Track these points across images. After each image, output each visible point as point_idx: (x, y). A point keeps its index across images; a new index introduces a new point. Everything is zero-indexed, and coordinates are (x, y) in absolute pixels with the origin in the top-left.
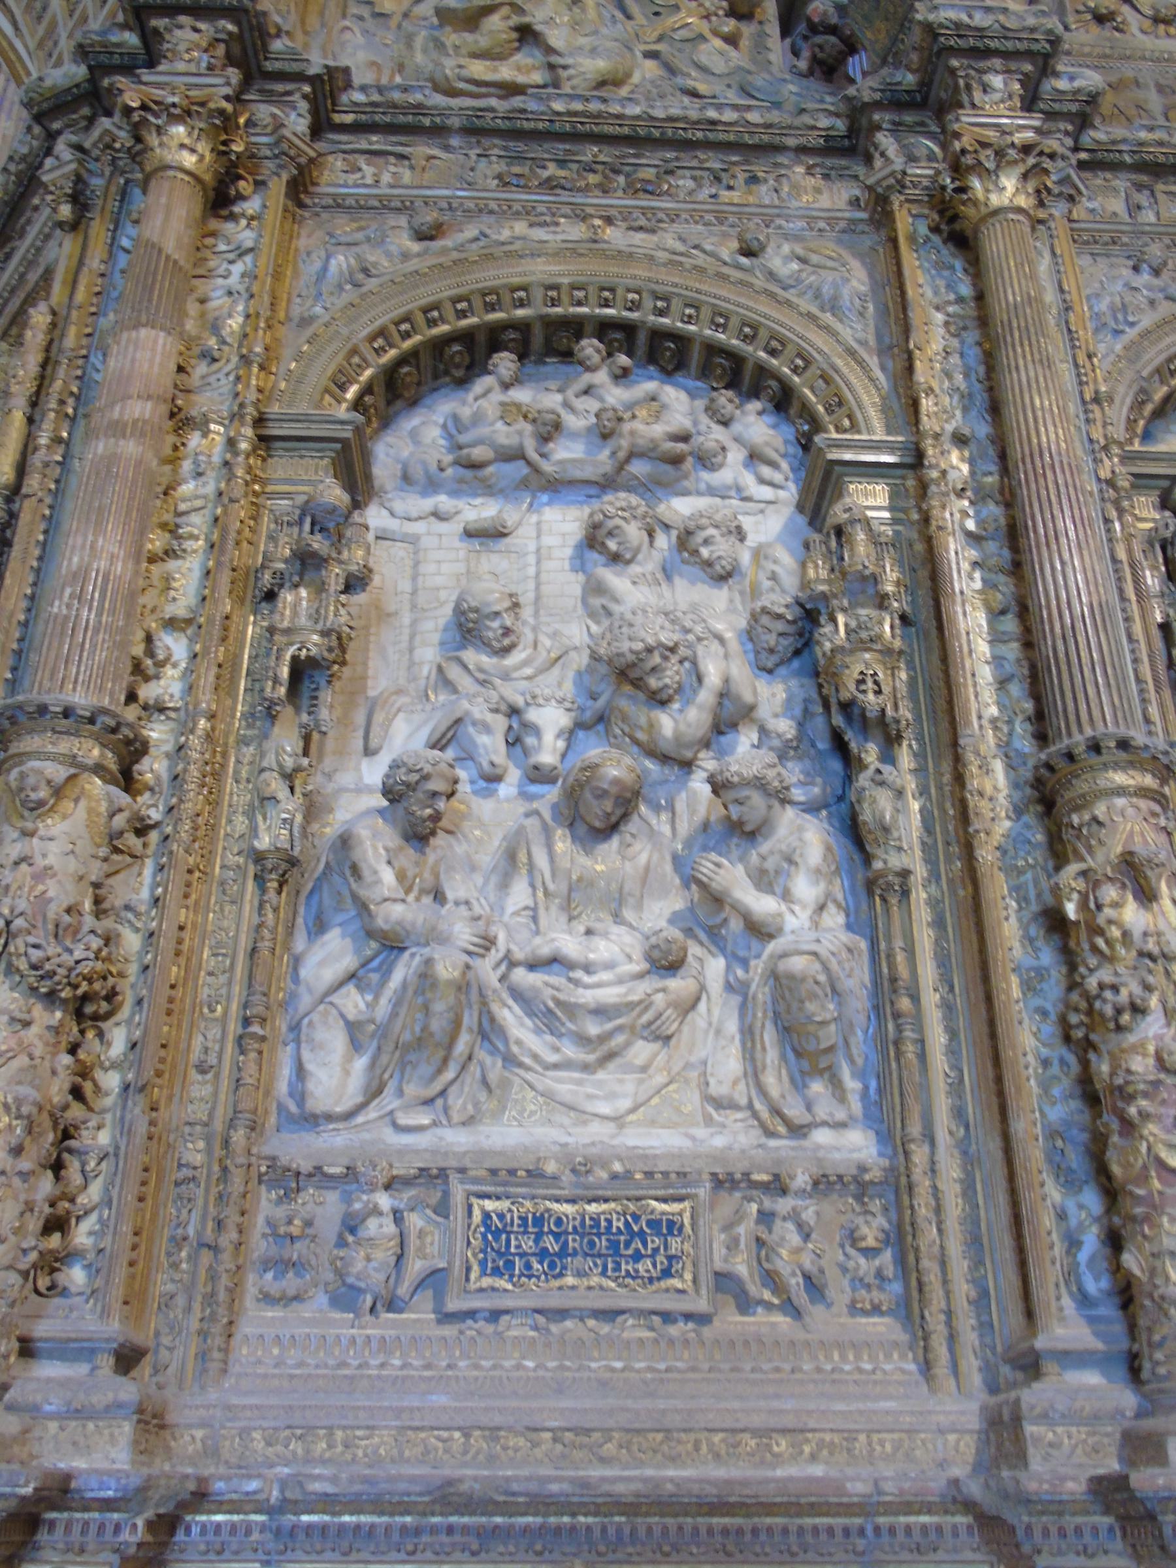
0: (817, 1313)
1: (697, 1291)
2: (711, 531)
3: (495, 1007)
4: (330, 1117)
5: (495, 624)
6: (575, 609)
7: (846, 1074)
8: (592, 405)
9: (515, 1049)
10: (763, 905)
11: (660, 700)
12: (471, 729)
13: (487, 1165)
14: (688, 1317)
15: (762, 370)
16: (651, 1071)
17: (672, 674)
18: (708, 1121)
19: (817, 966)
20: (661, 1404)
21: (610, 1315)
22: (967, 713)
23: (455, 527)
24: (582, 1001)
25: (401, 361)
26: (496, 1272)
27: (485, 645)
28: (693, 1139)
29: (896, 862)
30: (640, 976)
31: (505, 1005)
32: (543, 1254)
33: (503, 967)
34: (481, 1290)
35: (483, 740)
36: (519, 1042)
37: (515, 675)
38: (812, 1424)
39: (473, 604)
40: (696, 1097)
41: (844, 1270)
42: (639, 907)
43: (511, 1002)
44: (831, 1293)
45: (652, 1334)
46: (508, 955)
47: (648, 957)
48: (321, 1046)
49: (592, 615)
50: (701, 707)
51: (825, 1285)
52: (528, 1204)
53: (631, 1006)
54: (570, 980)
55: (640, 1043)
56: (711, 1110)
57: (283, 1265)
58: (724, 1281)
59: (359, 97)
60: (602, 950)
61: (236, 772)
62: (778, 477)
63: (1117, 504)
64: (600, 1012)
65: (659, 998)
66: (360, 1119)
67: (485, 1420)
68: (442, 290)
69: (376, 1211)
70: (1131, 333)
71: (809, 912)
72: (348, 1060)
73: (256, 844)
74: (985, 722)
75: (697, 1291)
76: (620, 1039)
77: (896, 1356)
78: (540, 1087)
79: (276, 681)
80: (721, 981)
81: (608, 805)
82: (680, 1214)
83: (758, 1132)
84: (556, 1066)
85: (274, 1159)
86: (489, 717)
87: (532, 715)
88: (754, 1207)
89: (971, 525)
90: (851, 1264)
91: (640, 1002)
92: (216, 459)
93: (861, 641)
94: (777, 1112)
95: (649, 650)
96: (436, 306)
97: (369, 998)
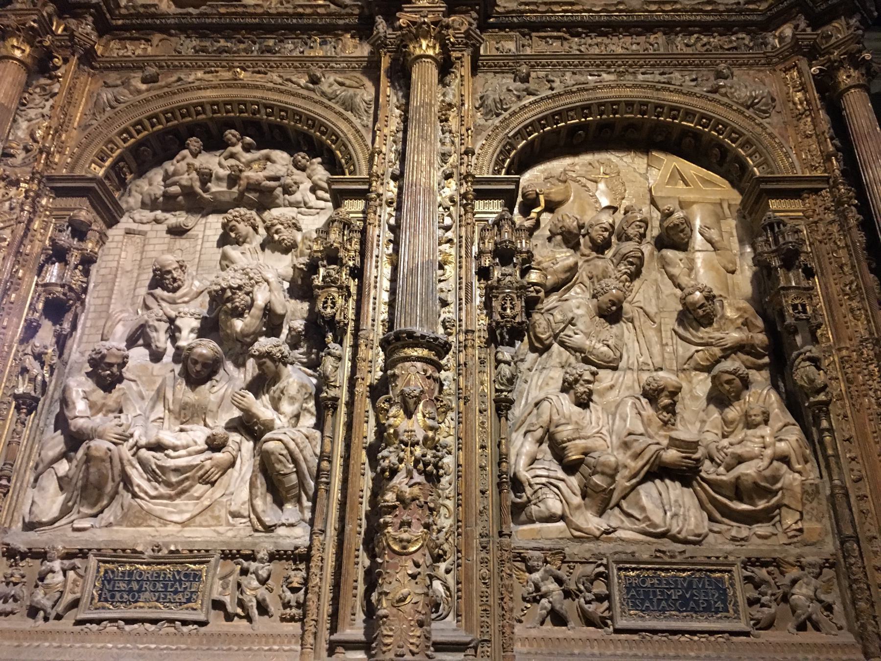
2: (279, 226)
3: (129, 469)
4: (41, 524)
5: (169, 276)
6: (216, 267)
7: (304, 498)
8: (232, 162)
9: (136, 489)
11: (239, 313)
12: (148, 330)
14: (195, 622)
16: (202, 499)
17: (241, 299)
18: (228, 524)
19: (282, 446)
21: (154, 622)
23: (164, 227)
24: (168, 465)
26: (106, 601)
27: (165, 288)
28: (218, 533)
29: (332, 393)
30: (202, 452)
31: (134, 467)
32: (130, 591)
33: (135, 449)
35: (153, 334)
36: (139, 486)
37: (179, 301)
40: (223, 513)
43: (138, 466)
44: (271, 609)
46: (136, 444)
47: (206, 443)
48: (43, 489)
51: (267, 606)
52: (128, 568)
54: (166, 455)
56: (230, 518)
58: (218, 605)
59: (123, 11)
61: (15, 355)
63: (465, 206)
64: (177, 470)
65: (208, 464)
66: (56, 525)
68: (157, 107)
69: (52, 571)
70: (506, 114)
75: (202, 609)
76: (187, 484)
77: (293, 641)
78: (145, 507)
81: (198, 367)
83: (250, 529)
85: (8, 545)
86: (156, 324)
87: (178, 322)
88: (239, 567)
91: (198, 465)
93: (329, 282)
94: (259, 520)
95: (223, 290)
96: (156, 116)
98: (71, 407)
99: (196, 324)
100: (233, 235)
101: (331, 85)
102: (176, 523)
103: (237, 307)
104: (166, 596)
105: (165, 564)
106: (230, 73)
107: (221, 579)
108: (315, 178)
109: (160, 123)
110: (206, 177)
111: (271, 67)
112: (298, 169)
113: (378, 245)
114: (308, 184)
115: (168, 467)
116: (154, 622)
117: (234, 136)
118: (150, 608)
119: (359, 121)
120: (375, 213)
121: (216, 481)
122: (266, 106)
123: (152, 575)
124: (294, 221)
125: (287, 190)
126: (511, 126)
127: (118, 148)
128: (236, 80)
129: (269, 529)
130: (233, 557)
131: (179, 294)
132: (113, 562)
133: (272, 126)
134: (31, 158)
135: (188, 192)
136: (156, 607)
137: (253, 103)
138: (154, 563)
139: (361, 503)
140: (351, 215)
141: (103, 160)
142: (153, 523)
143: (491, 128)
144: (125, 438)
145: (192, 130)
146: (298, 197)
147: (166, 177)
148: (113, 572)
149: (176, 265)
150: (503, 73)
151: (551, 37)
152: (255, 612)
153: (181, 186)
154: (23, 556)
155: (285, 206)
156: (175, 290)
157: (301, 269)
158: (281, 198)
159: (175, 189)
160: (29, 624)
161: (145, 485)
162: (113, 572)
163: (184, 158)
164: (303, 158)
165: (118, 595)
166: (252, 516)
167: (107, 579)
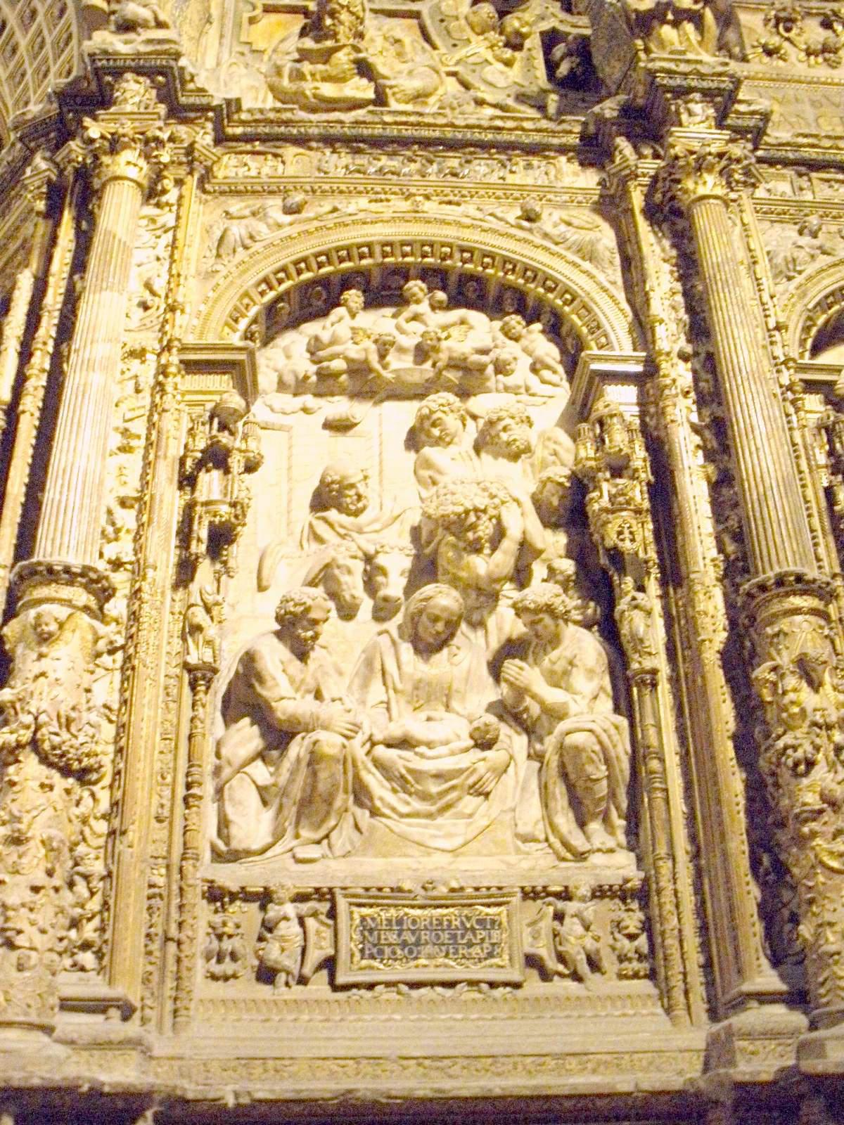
0: (593, 978)
1: (512, 966)
4: (248, 853)
5: (352, 492)
7: (614, 814)
8: (416, 327)
9: (378, 803)
10: (553, 696)
11: (476, 548)
12: (337, 572)
14: (506, 984)
15: (540, 301)
16: (477, 816)
17: (486, 529)
18: (518, 851)
19: (594, 739)
20: (490, 1041)
21: (451, 985)
22: (695, 555)
25: (279, 299)
26: (372, 957)
27: (342, 509)
28: (509, 864)
29: (648, 664)
30: (467, 750)
31: (370, 772)
32: (404, 944)
33: (368, 745)
34: (361, 969)
35: (344, 578)
36: (381, 799)
38: (593, 1049)
39: (337, 478)
40: (508, 836)
41: (614, 949)
42: (463, 699)
43: (374, 770)
45: (481, 996)
46: (370, 738)
47: (472, 737)
49: (420, 481)
51: (600, 959)
54: (416, 754)
55: (469, 797)
56: (519, 843)
58: (532, 961)
59: (244, 116)
61: (172, 607)
62: (555, 378)
63: (793, 402)
64: (438, 776)
65: (482, 768)
66: (269, 854)
67: (369, 1053)
68: (306, 248)
69: (286, 918)
71: (587, 701)
74: (708, 561)
75: (512, 966)
77: (649, 1003)
78: (396, 829)
80: (525, 754)
82: (499, 915)
84: (408, 816)
87: (381, 560)
88: (551, 909)
90: (618, 945)
91: (468, 769)
94: (565, 844)
95: (467, 512)
96: (305, 260)
97: (272, 769)
98: (270, 683)
102: (443, 851)
104: (457, 950)
105: (447, 907)
106: (409, 202)
107: (529, 925)
109: (308, 269)
111: (463, 196)
112: (511, 338)
116: (451, 985)
117: (421, 290)
118: (437, 966)
123: (431, 923)
125: (501, 368)
126: (810, 295)
127: (255, 304)
128: (417, 212)
129: (580, 856)
131: (363, 519)
132: (371, 906)
133: (467, 278)
135: (359, 370)
138: (430, 906)
141: (236, 321)
142: (410, 851)
143: (785, 297)
145: (346, 282)
147: (315, 347)
149: (360, 477)
150: (781, 222)
151: (837, 181)
152: (584, 968)
153: (347, 359)
154: (233, 897)
155: (497, 391)
156: (356, 513)
157: (561, 484)
158: (493, 380)
162: (373, 919)
163: (340, 320)
165: (387, 950)
167: (367, 928)
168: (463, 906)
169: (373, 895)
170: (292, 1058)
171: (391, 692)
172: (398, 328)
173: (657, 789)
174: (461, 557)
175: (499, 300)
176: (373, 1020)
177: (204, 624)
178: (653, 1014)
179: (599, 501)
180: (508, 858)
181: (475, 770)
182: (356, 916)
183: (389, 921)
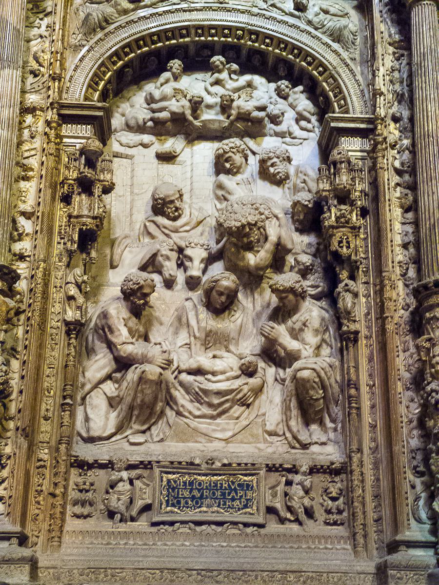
0: (309, 523)
1: (258, 514)
2: (275, 160)
3: (173, 391)
4: (100, 439)
5: (172, 206)
6: (209, 196)
8: (217, 89)
9: (181, 409)
10: (293, 345)
11: (249, 247)
12: (160, 259)
13: (169, 460)
14: (254, 525)
15: (302, 70)
16: (241, 419)
17: (255, 236)
18: (265, 441)
19: (315, 374)
20: (242, 560)
21: (220, 524)
22: (387, 260)
23: (151, 152)
24: (210, 388)
26: (173, 505)
28: (259, 449)
29: (353, 327)
31: (176, 389)
32: (193, 498)
33: (176, 373)
34: (167, 513)
36: (183, 406)
37: (181, 230)
39: (161, 196)
40: (260, 431)
42: (237, 344)
43: (179, 388)
44: (317, 515)
45: (239, 532)
47: (240, 368)
48: (96, 407)
49: (218, 198)
50: (266, 251)
51: (314, 512)
53: (232, 391)
54: (206, 379)
55: (236, 406)
56: (267, 436)
57: (83, 503)
58: (271, 510)
60: (219, 365)
62: (310, 126)
64: (219, 393)
65: (246, 389)
66: (114, 439)
67: (169, 566)
71: (313, 349)
72: (107, 413)
73: (66, 318)
74: (396, 264)
75: (258, 514)
76: (227, 405)
77: (342, 542)
78: (192, 426)
79: (73, 242)
80: (273, 378)
81: (223, 298)
82: (252, 481)
83: (288, 446)
84: (199, 417)
86: (169, 253)
87: (188, 252)
88: (284, 479)
89: (397, 164)
92: (40, 129)
93: (342, 222)
95: (243, 226)
97: (117, 386)
98: (116, 333)
99: (205, 254)
100: (228, 165)
101: (317, 15)
102: (220, 439)
103: (251, 242)
105: (220, 475)
107: (270, 488)
108: (300, 108)
109: (145, 45)
110: (196, 105)
112: (281, 97)
113: (389, 189)
114: (290, 115)
115: (211, 391)
116: (220, 524)
117: (222, 63)
118: (213, 512)
119: (347, 53)
120: (384, 157)
121: (251, 403)
122: (251, 32)
123: (210, 485)
124: (287, 155)
125: (275, 120)
127: (109, 71)
129: (305, 446)
130: (277, 470)
131: (179, 223)
132: (174, 473)
133: (254, 52)
134: (40, 84)
136: (218, 512)
137: (238, 29)
138: (210, 474)
139: (402, 427)
140: (350, 153)
142: (199, 439)
144: (170, 362)
145: (172, 53)
146: (283, 127)
147: (150, 100)
148: (175, 482)
149: (178, 196)
152: (303, 517)
153: (173, 114)
154: (91, 466)
155: (271, 136)
156: (175, 219)
159: (164, 115)
160: (107, 525)
161: (189, 406)
163: (167, 81)
164: (287, 87)
165: (182, 501)
166: (288, 435)
168: (230, 475)
169: (174, 466)
170: (121, 568)
171: (192, 338)
172: (206, 90)
173: (353, 407)
174: (239, 252)
175: (275, 68)
176: (172, 545)
177: (76, 296)
178: (344, 549)
179: (331, 217)
180: (259, 445)
181: (241, 390)
182: (165, 479)
183: (185, 483)
